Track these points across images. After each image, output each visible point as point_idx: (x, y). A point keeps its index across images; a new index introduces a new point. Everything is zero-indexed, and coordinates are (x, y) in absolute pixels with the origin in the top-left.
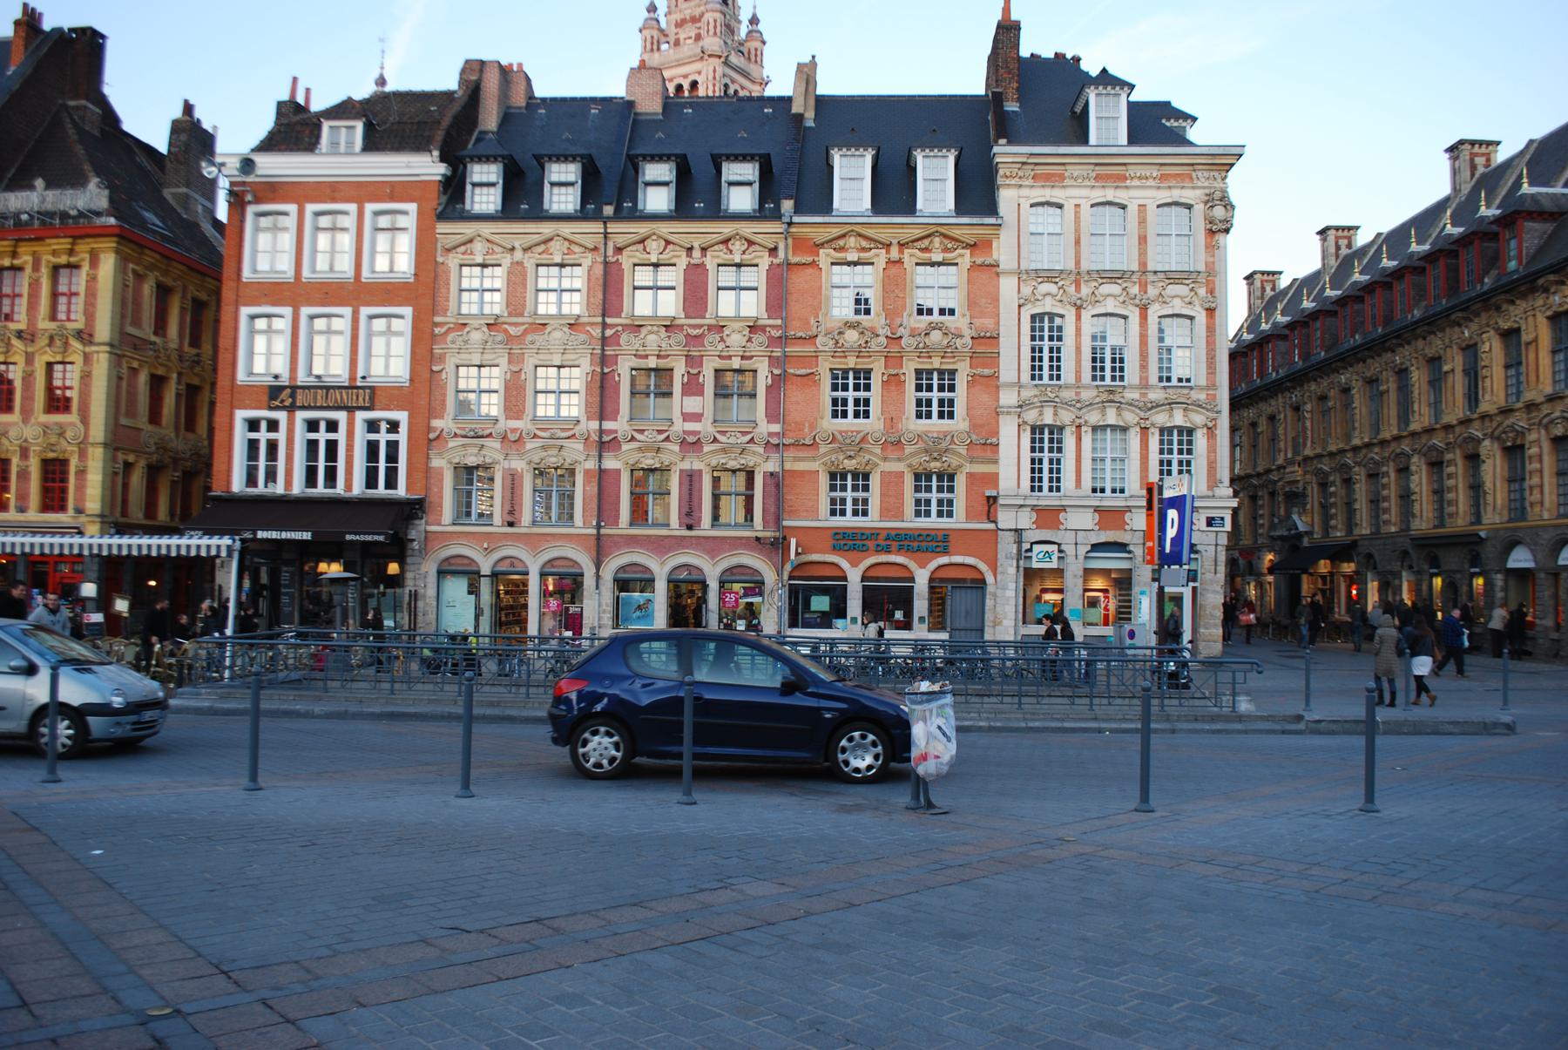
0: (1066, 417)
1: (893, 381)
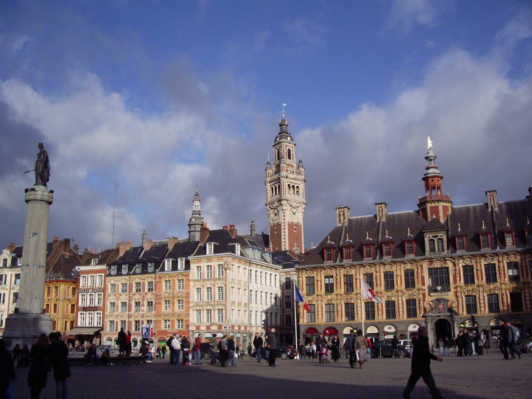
0: (201, 308)
1: (173, 303)
